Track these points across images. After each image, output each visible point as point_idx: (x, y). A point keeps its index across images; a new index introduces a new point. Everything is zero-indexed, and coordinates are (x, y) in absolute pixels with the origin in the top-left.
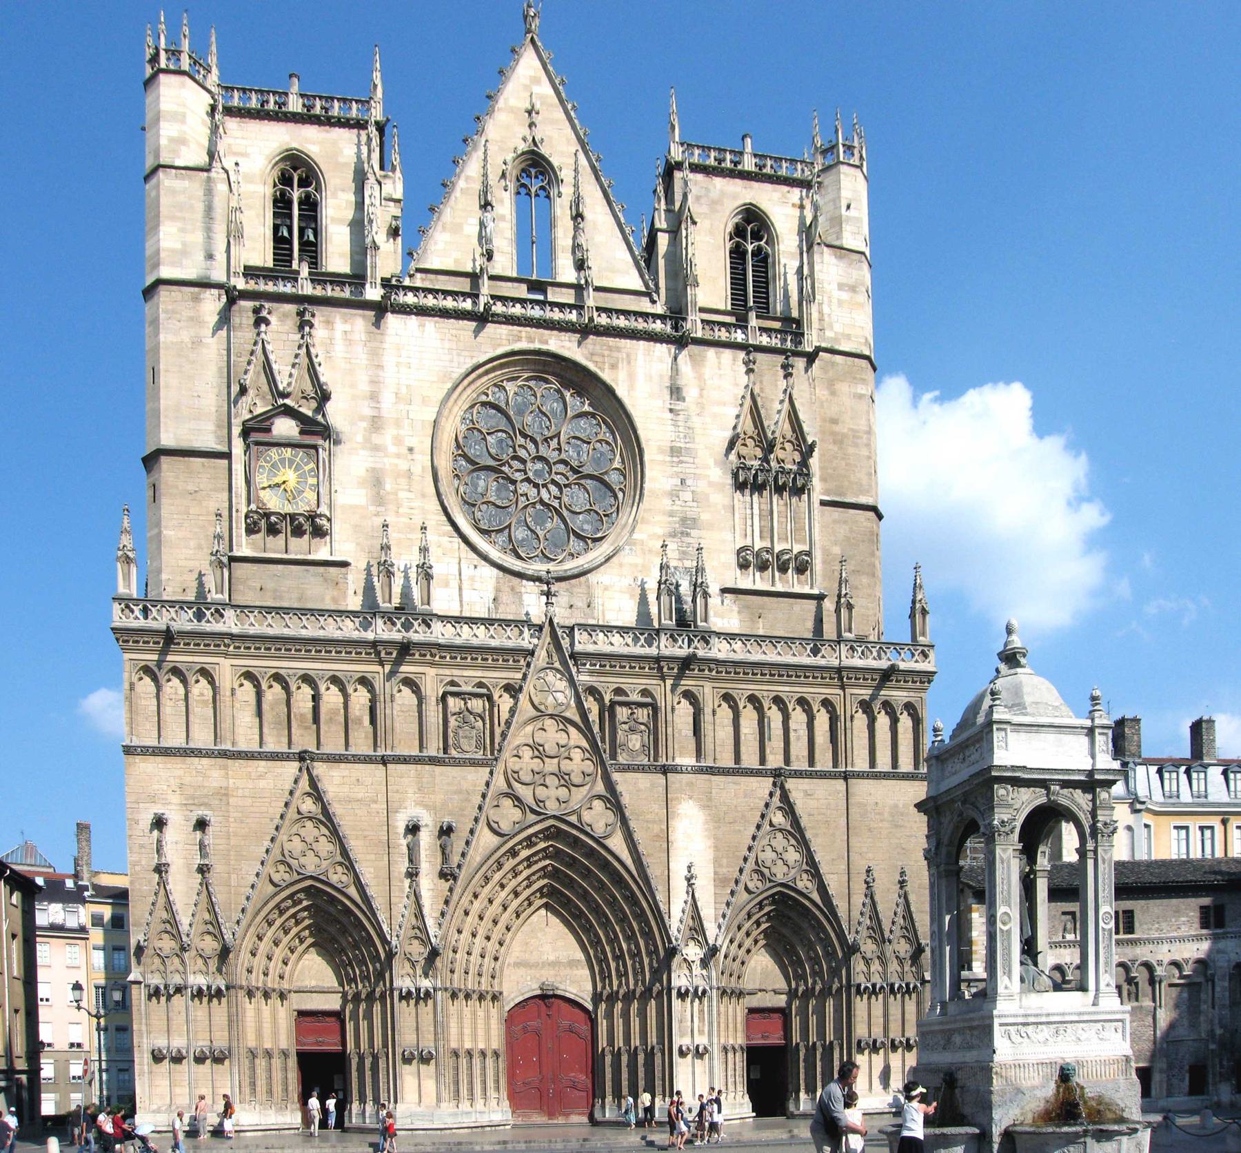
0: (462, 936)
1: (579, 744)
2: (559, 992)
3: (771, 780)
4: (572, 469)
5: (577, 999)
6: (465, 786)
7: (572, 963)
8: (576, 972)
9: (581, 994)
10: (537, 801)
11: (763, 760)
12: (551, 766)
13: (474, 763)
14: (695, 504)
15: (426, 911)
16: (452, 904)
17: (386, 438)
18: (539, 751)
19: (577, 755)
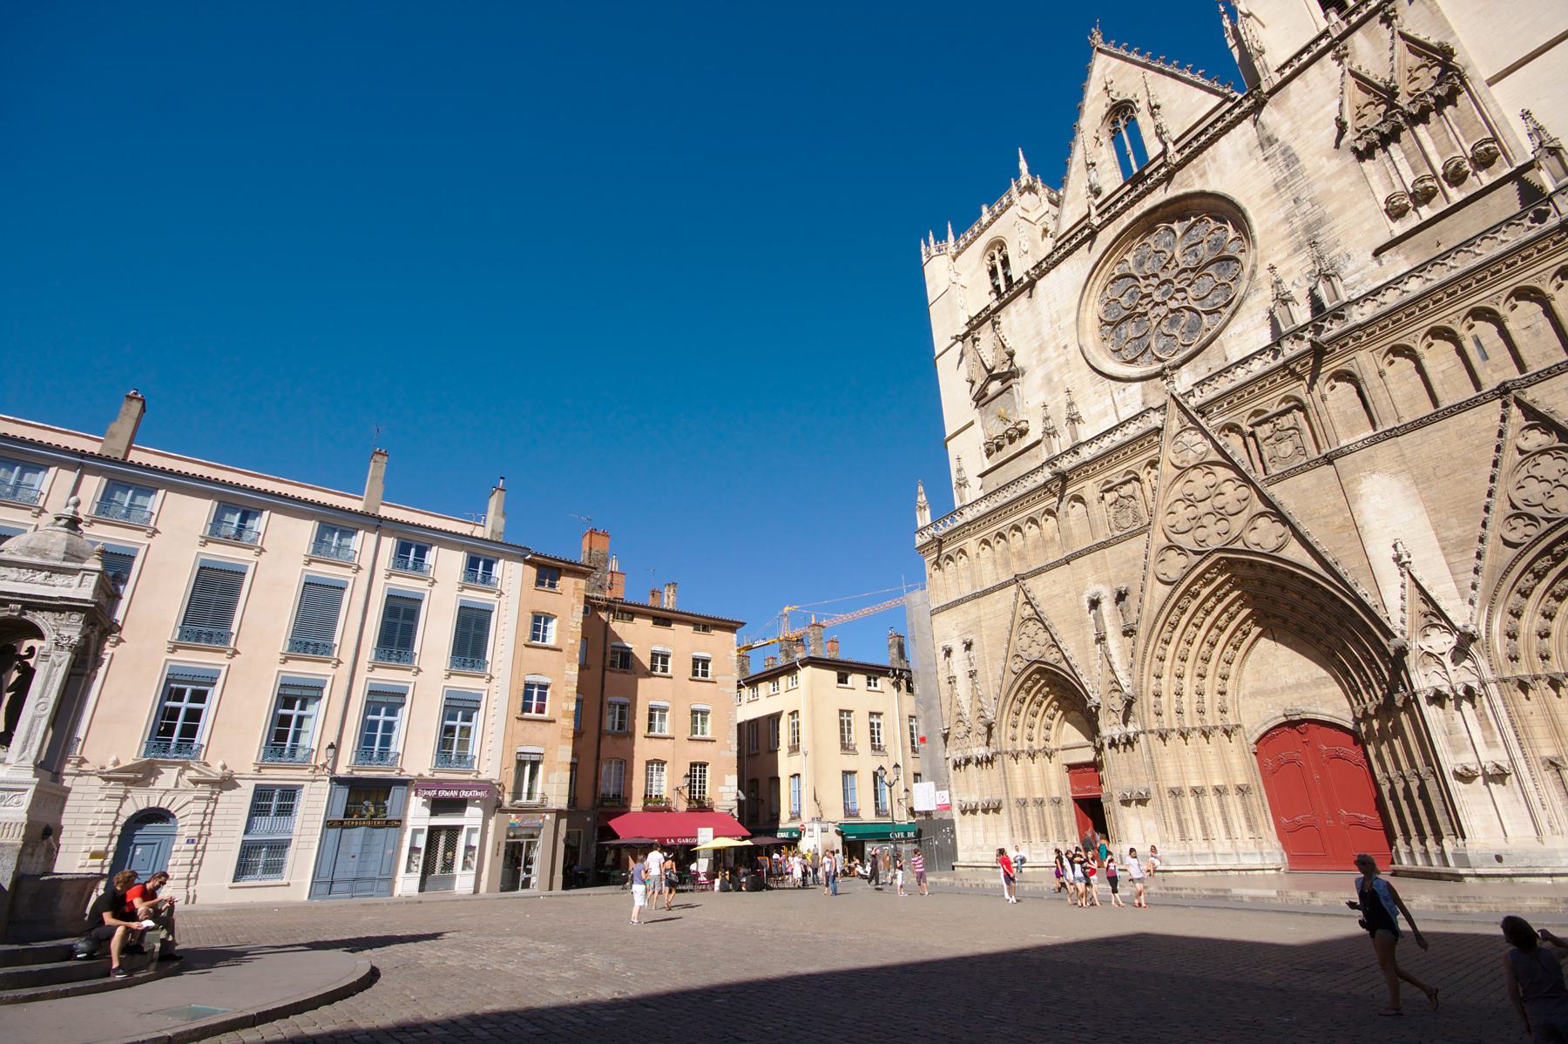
0: (1162, 680)
1: (1228, 477)
2: (1309, 716)
3: (1499, 402)
4: (1192, 270)
5: (1334, 720)
6: (1130, 554)
7: (1317, 683)
8: (1324, 691)
9: (1340, 714)
10: (1200, 542)
11: (1477, 385)
12: (1203, 508)
13: (1133, 535)
14: (1317, 207)
15: (1116, 667)
16: (1139, 655)
17: (1050, 351)
18: (1190, 501)
19: (1228, 488)
